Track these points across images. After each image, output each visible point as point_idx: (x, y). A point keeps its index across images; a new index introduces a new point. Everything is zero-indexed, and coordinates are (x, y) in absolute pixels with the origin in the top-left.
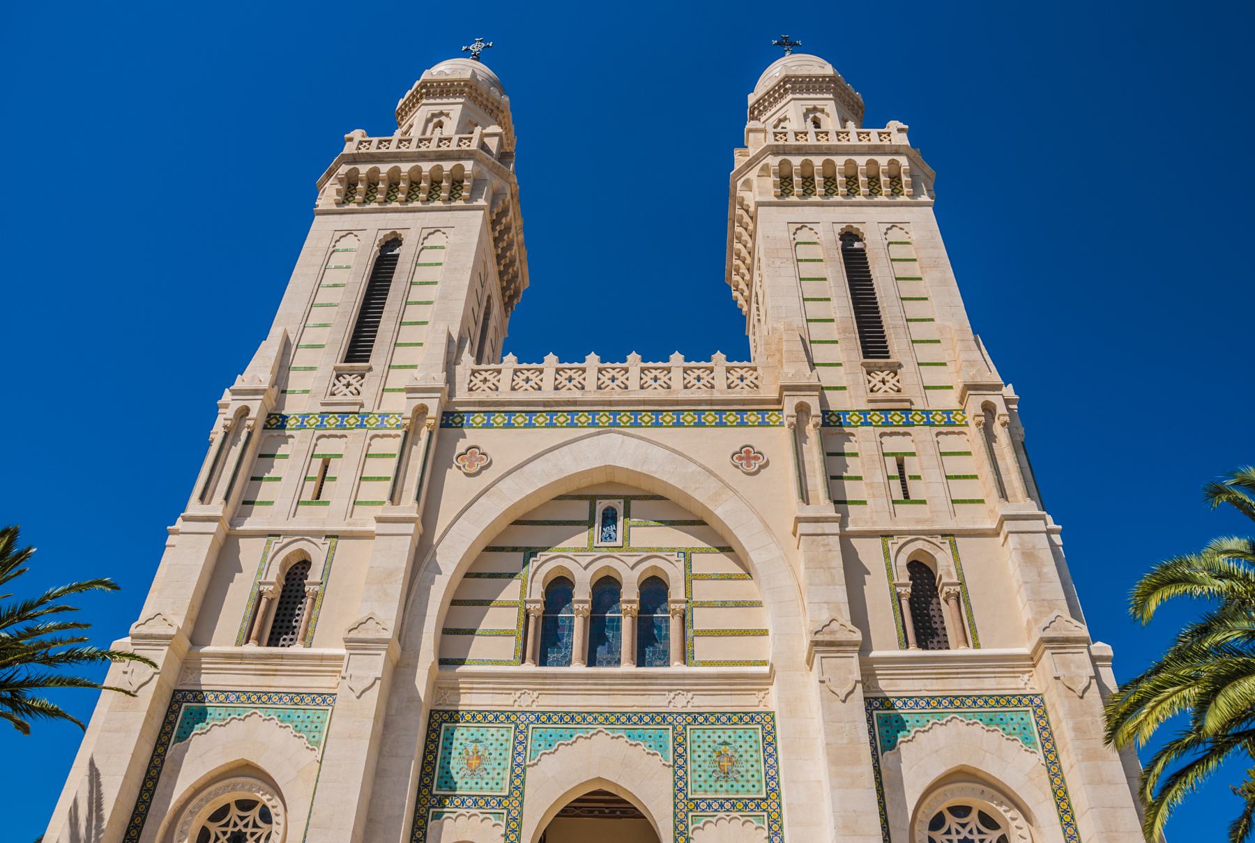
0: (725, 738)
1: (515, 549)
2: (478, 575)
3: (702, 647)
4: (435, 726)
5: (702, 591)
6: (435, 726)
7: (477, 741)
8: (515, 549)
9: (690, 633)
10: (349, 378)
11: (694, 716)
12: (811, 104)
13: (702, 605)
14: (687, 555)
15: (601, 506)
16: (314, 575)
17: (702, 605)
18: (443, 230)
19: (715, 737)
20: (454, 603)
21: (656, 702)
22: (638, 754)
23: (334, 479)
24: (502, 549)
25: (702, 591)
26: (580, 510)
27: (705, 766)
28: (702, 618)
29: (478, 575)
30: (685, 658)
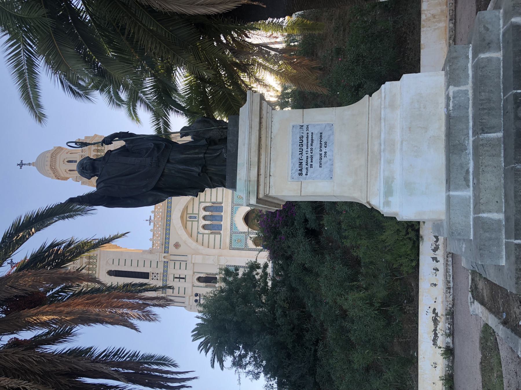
0: (236, 197)
1: (197, 236)
2: (203, 243)
3: (219, 200)
4: (232, 249)
5: (208, 200)
6: (232, 249)
7: (235, 241)
8: (197, 236)
9: (216, 202)
10: (153, 276)
11: (232, 202)
12: (62, 162)
13: (211, 200)
14: (200, 202)
15: (188, 219)
16: (202, 275)
17: (211, 200)
18: (107, 260)
19: (236, 199)
20: (208, 247)
21: (229, 209)
22: (238, 212)
23: (180, 275)
24: (197, 239)
25: (208, 200)
26: (189, 224)
27: (241, 200)
28: (214, 200)
29: (203, 243)
30: (221, 203)
